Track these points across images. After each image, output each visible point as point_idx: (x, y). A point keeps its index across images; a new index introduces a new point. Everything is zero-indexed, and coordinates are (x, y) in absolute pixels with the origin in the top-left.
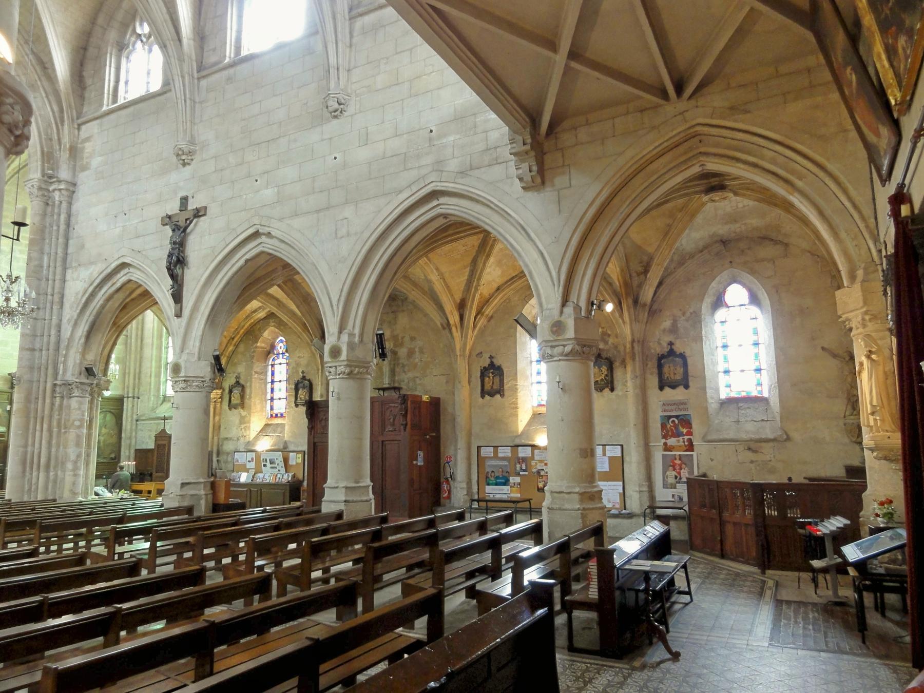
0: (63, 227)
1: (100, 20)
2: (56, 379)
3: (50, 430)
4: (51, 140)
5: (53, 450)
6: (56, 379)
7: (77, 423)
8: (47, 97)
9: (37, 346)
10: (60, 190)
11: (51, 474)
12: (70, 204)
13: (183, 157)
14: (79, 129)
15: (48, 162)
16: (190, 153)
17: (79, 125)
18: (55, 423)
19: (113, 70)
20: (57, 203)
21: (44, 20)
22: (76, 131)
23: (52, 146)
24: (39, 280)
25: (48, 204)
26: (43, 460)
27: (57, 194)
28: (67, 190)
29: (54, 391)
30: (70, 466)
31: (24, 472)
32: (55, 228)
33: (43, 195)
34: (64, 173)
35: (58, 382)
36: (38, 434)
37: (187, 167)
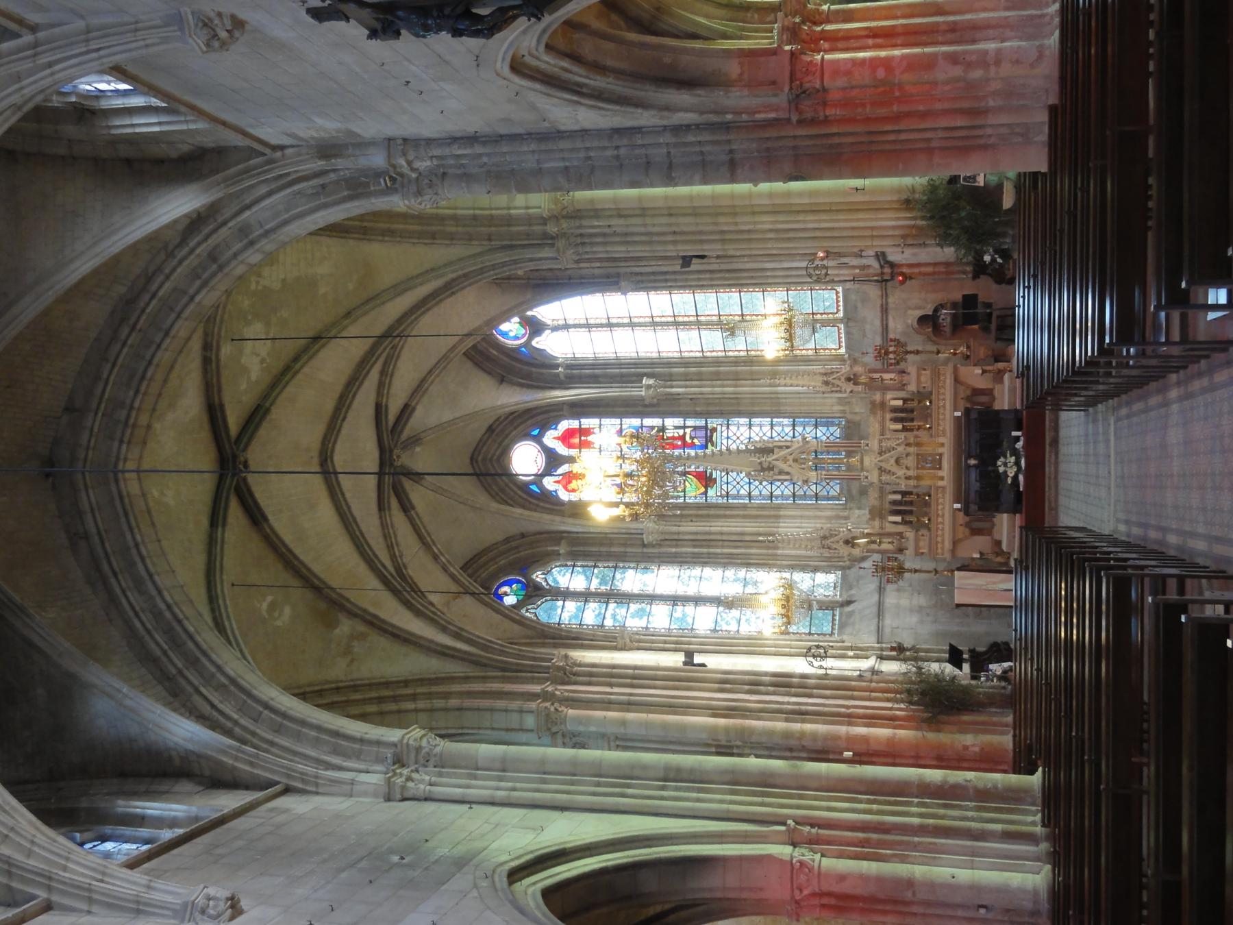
0: (479, 149)
1: (62, 151)
2: (789, 120)
3: (897, 118)
4: (323, 186)
5: (939, 106)
6: (789, 120)
7: (881, 73)
8: (248, 207)
9: (725, 158)
10: (409, 163)
11: (991, 103)
12: (429, 142)
13: (223, 34)
14: (282, 148)
15: (367, 185)
16: (206, 24)
17: (275, 148)
18: (882, 112)
19: (136, 121)
20: (435, 162)
21: (116, 249)
22: (289, 151)
23: (337, 182)
24: (593, 169)
25: (444, 174)
26: (960, 122)
27: (417, 164)
28: (404, 154)
29: (813, 122)
30: (977, 74)
31: (984, 147)
32: (485, 159)
33: (430, 186)
34: (378, 160)
35: (794, 118)
36: (903, 137)
37: (242, 15)
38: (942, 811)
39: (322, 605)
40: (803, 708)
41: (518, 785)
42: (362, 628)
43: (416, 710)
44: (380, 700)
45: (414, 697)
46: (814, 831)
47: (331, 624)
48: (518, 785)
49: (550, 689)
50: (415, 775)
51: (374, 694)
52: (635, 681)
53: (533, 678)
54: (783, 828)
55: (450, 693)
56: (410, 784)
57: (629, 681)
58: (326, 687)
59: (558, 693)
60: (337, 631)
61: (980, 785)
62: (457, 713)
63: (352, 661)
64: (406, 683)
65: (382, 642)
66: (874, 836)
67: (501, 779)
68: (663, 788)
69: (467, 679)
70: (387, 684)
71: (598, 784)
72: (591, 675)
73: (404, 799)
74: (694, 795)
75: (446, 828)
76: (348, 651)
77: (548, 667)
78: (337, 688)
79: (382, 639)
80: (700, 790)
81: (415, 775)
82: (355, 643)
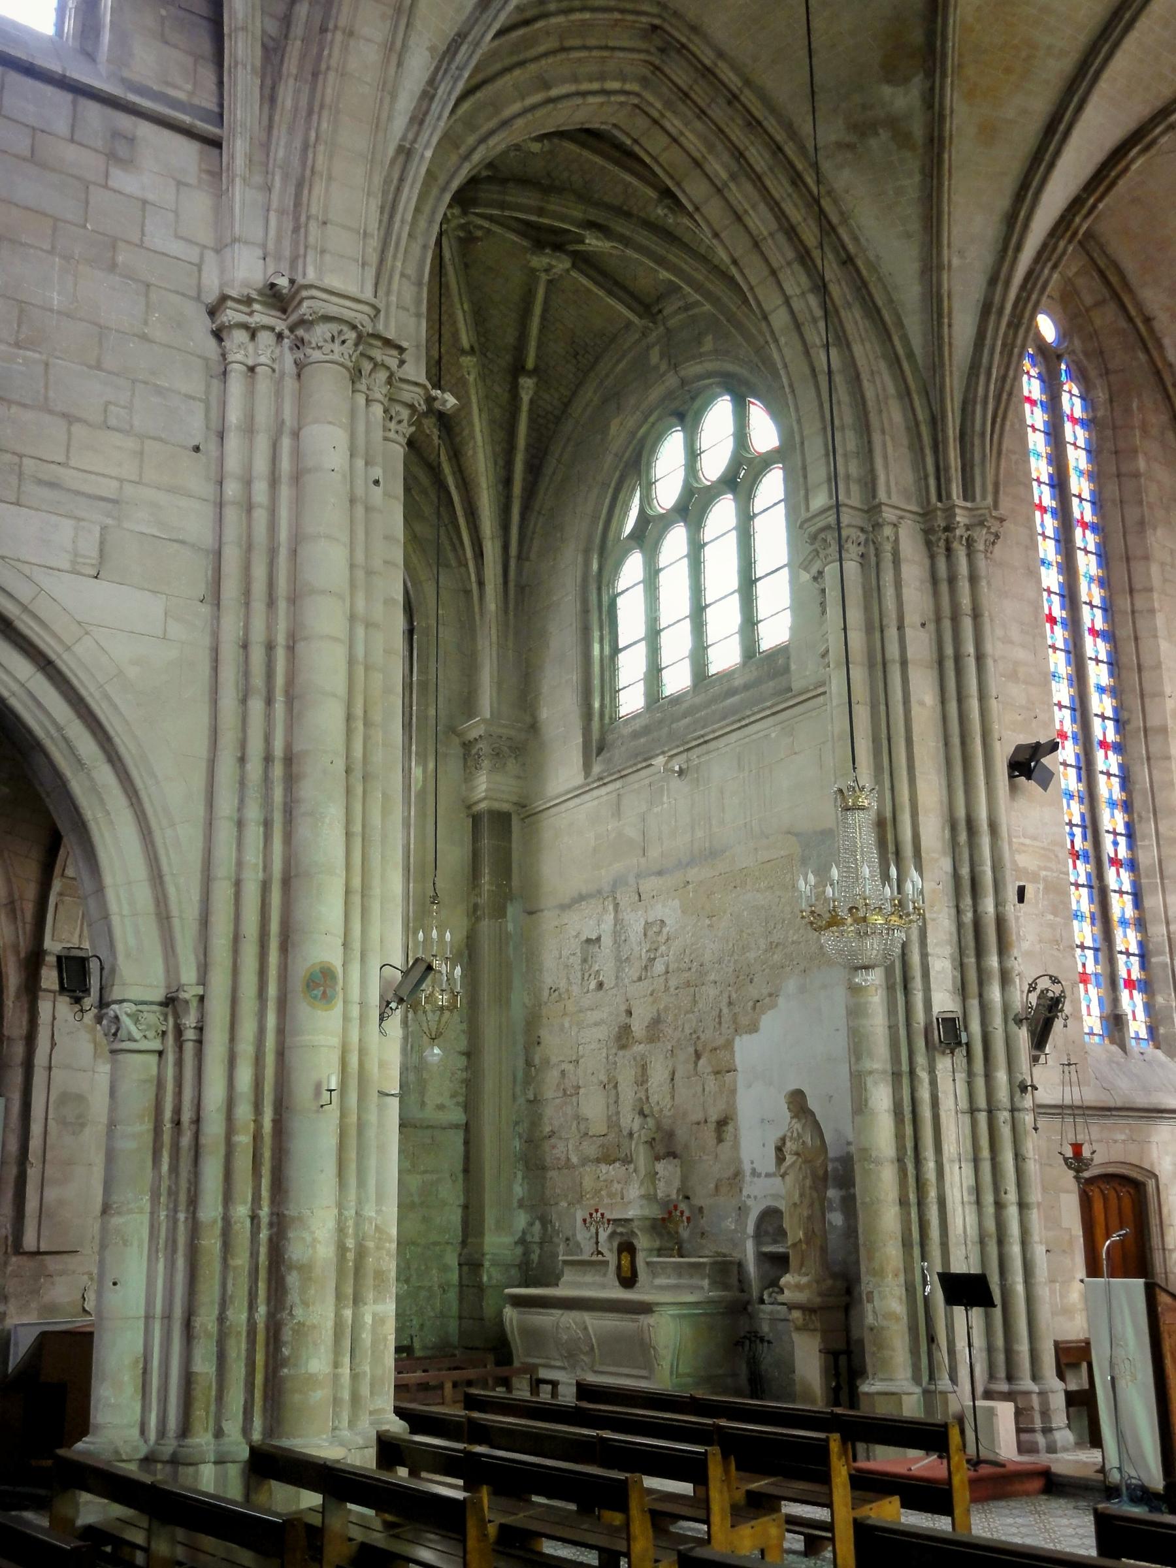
38: (241, 1260)
39: (917, 36)
40: (917, 983)
41: (260, 517)
42: (918, 130)
43: (787, 301)
44: (791, 232)
45: (821, 288)
46: (190, 1034)
47: (891, 73)
48: (260, 517)
49: (888, 515)
50: (265, 338)
51: (795, 214)
52: (950, 665)
53: (926, 477)
54: (188, 975)
55: (849, 346)
56: (240, 336)
57: (949, 651)
58: (771, 124)
59: (888, 531)
60: (887, 90)
61: (287, 1334)
62: (807, 371)
63: (850, 147)
64: (848, 261)
65: (912, 183)
66: (186, 1140)
67: (274, 482)
68: (268, 759)
69: (895, 362)
70: (827, 228)
71: (270, 647)
72: (952, 580)
73: (218, 335)
74: (253, 813)
75: (70, 419)
76: (863, 129)
77: (949, 497)
78: (780, 149)
79: (917, 178)
80: (267, 824)
81: (265, 338)
82: (884, 135)
